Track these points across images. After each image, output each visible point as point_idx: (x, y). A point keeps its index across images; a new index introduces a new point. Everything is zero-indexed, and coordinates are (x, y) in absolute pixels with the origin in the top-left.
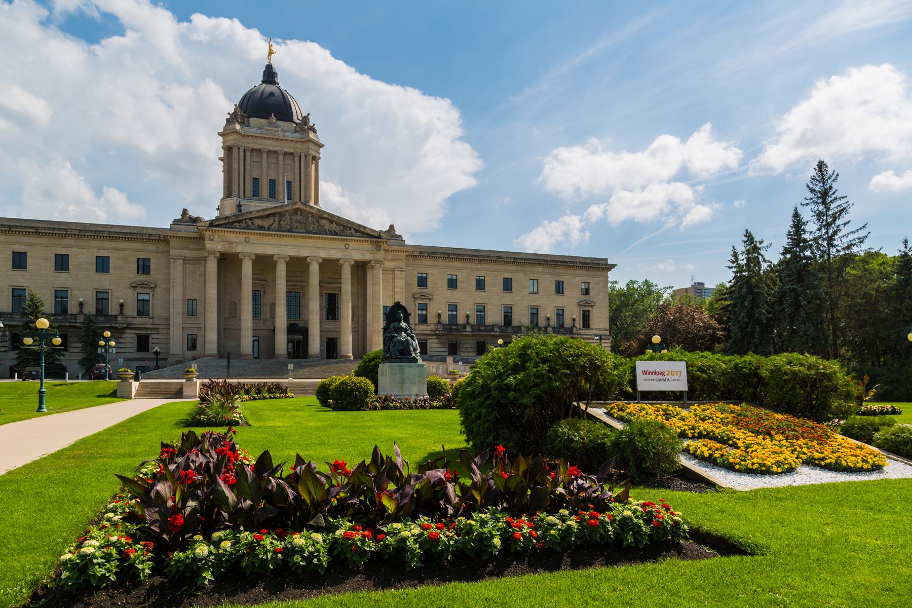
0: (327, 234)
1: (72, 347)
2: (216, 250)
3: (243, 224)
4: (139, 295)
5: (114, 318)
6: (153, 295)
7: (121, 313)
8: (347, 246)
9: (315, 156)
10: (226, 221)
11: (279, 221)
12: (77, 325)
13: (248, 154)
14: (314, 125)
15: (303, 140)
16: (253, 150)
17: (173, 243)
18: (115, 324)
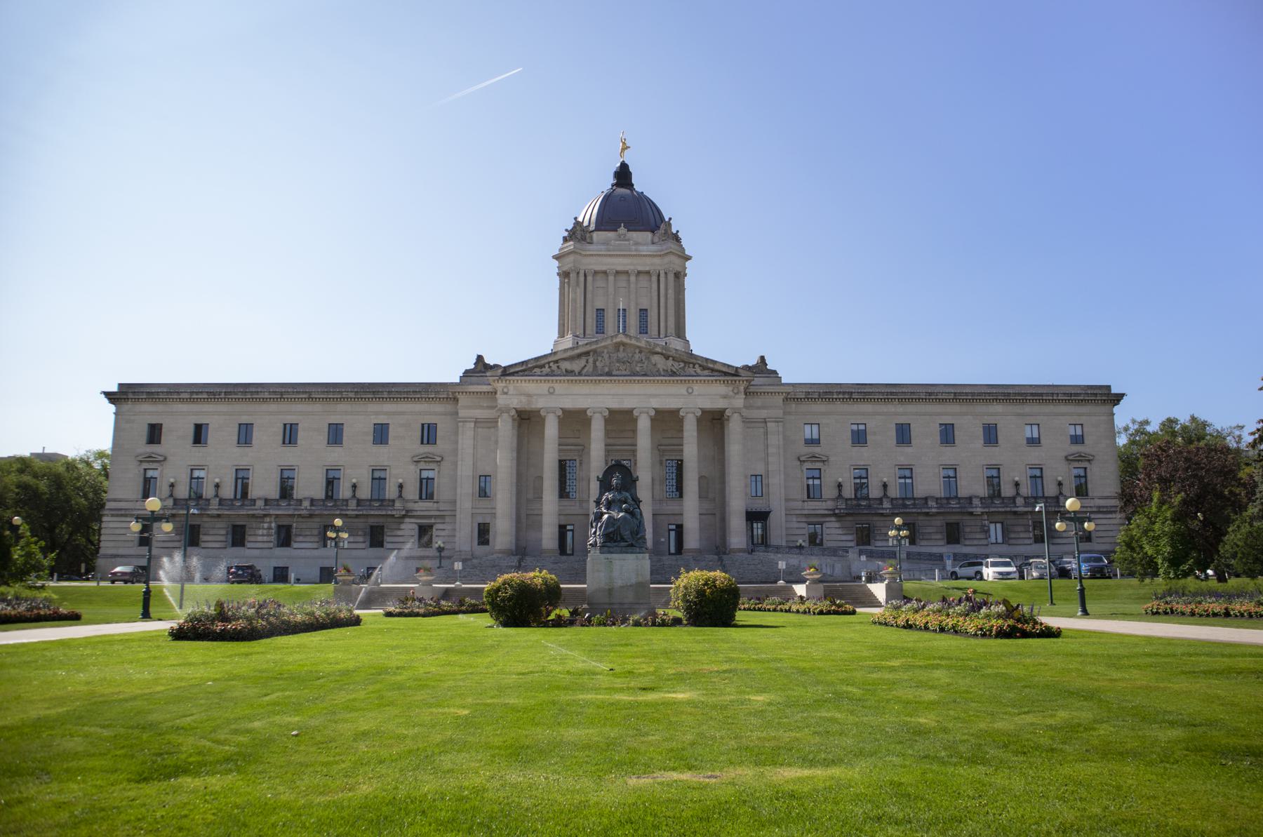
0: (660, 375)
1: (296, 542)
2: (512, 406)
3: (546, 370)
4: (423, 472)
5: (391, 503)
6: (439, 472)
7: (400, 496)
8: (690, 391)
10: (524, 367)
11: (595, 362)
12: (348, 513)
13: (590, 278)
14: (678, 231)
15: (663, 253)
16: (596, 273)
17: (463, 400)
18: (391, 510)
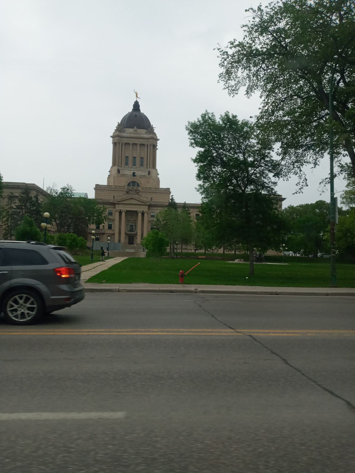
9: (155, 145)
13: (123, 145)
